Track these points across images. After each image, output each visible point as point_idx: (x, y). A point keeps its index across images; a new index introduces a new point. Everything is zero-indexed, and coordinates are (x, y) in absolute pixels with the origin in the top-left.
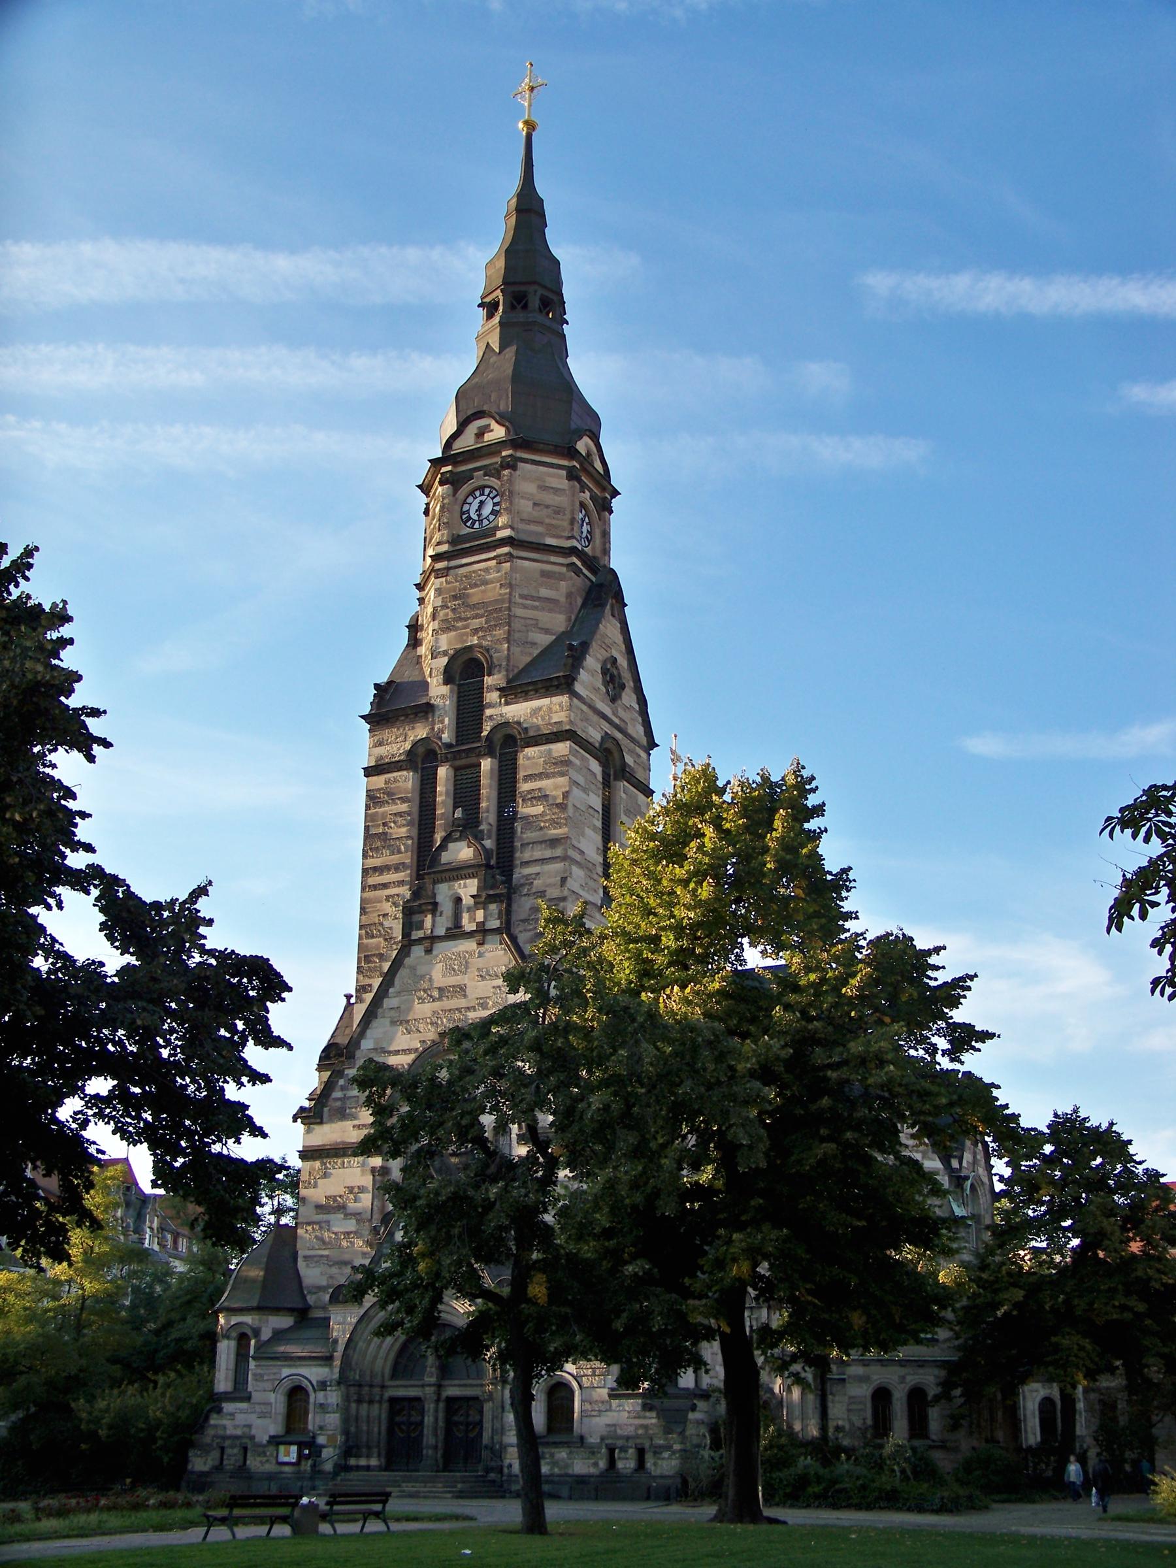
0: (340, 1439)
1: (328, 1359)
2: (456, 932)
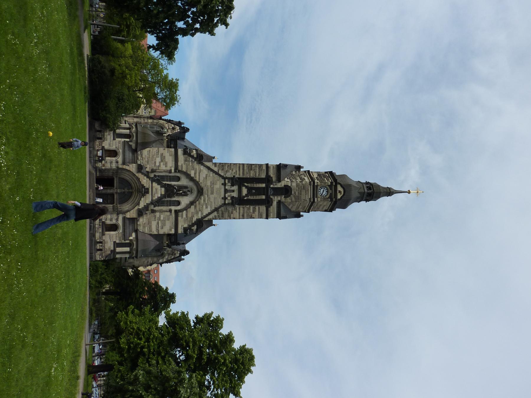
0: (103, 168)
1: (124, 163)
2: (226, 191)
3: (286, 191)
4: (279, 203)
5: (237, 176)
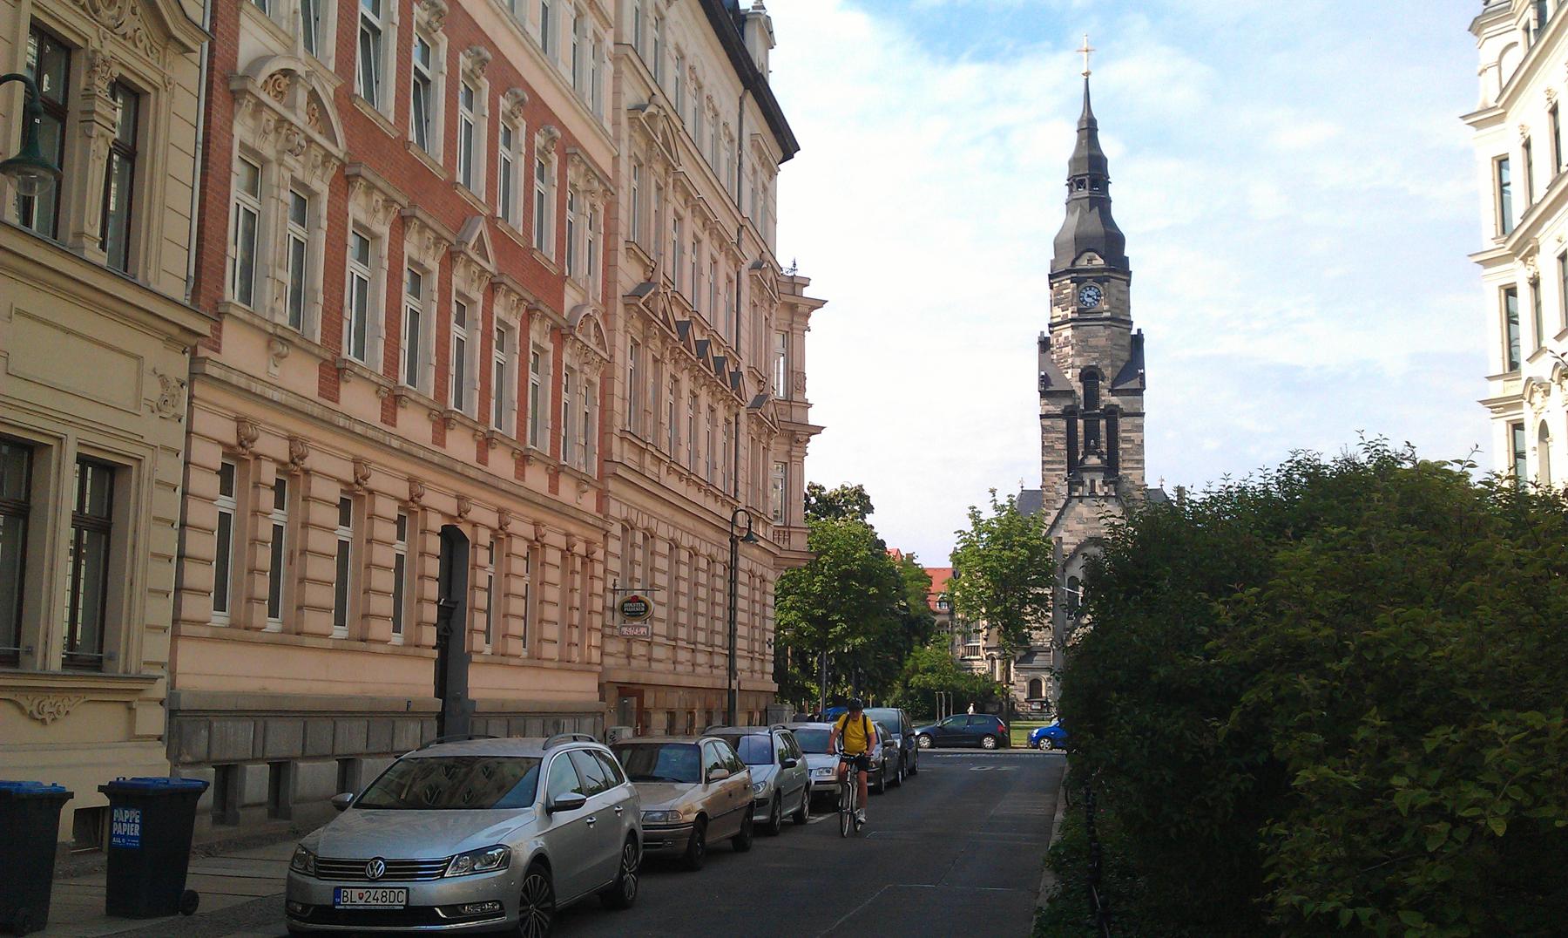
3: (1090, 376)
4: (1113, 392)
5: (1065, 473)
